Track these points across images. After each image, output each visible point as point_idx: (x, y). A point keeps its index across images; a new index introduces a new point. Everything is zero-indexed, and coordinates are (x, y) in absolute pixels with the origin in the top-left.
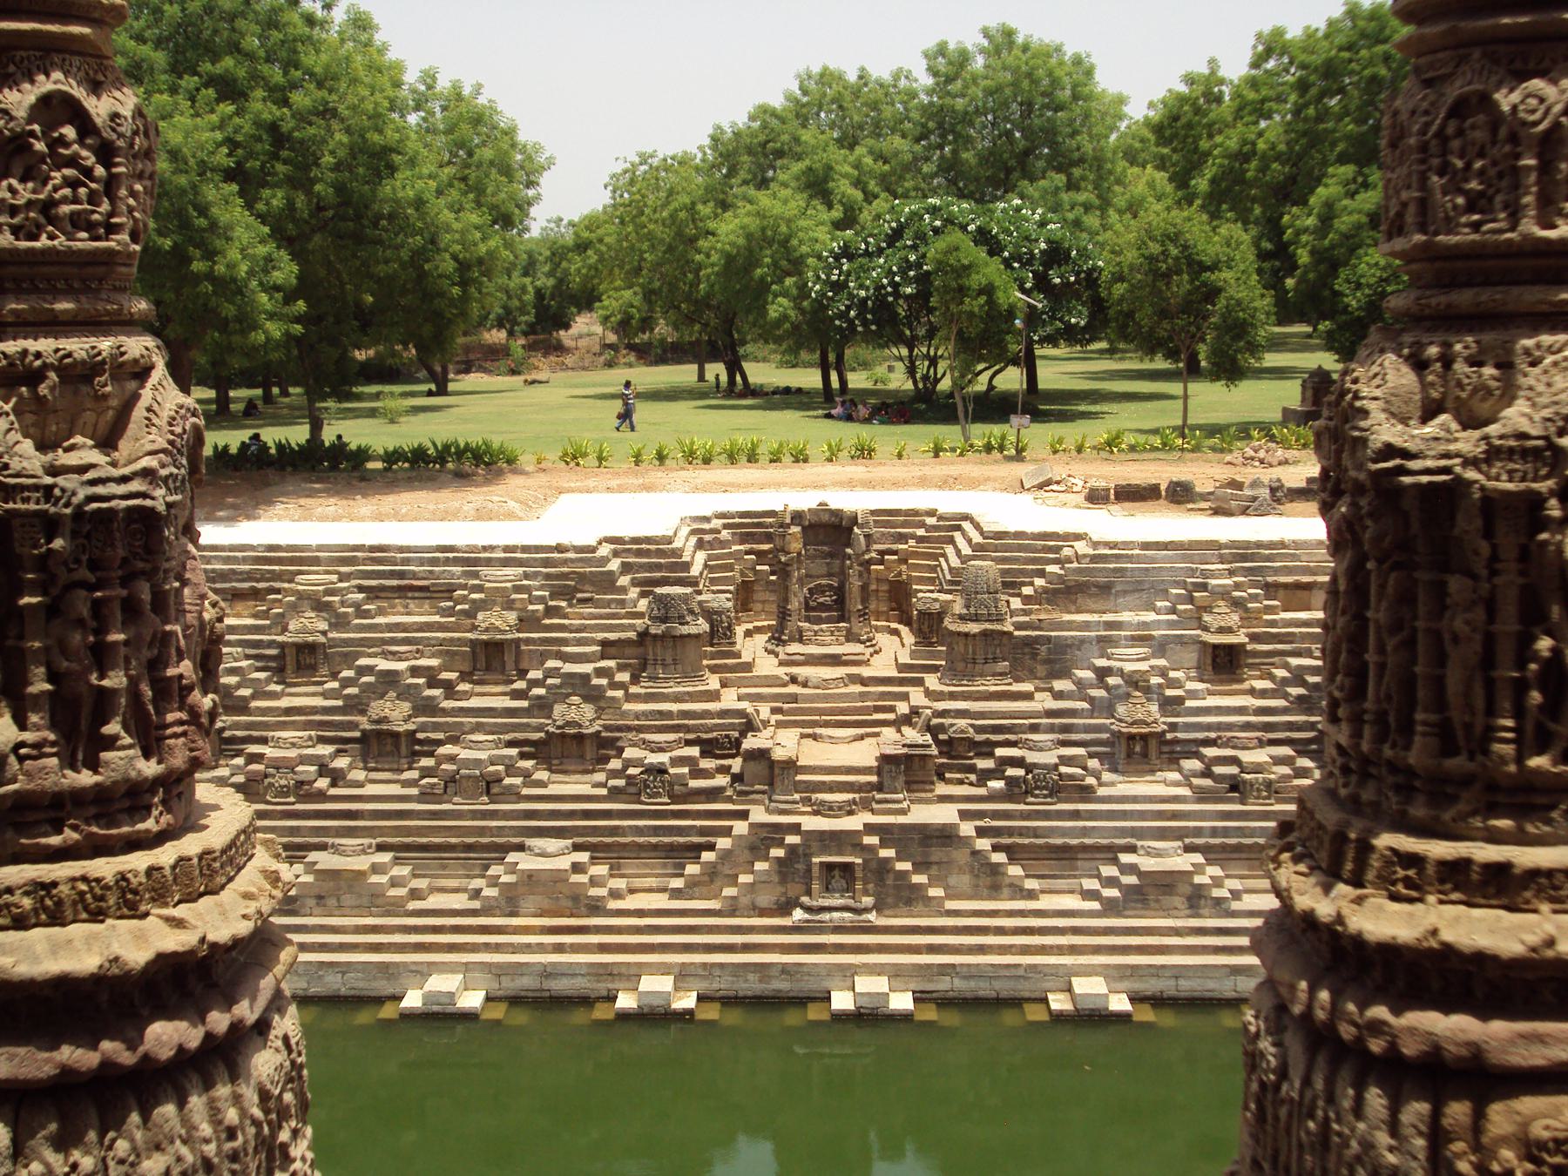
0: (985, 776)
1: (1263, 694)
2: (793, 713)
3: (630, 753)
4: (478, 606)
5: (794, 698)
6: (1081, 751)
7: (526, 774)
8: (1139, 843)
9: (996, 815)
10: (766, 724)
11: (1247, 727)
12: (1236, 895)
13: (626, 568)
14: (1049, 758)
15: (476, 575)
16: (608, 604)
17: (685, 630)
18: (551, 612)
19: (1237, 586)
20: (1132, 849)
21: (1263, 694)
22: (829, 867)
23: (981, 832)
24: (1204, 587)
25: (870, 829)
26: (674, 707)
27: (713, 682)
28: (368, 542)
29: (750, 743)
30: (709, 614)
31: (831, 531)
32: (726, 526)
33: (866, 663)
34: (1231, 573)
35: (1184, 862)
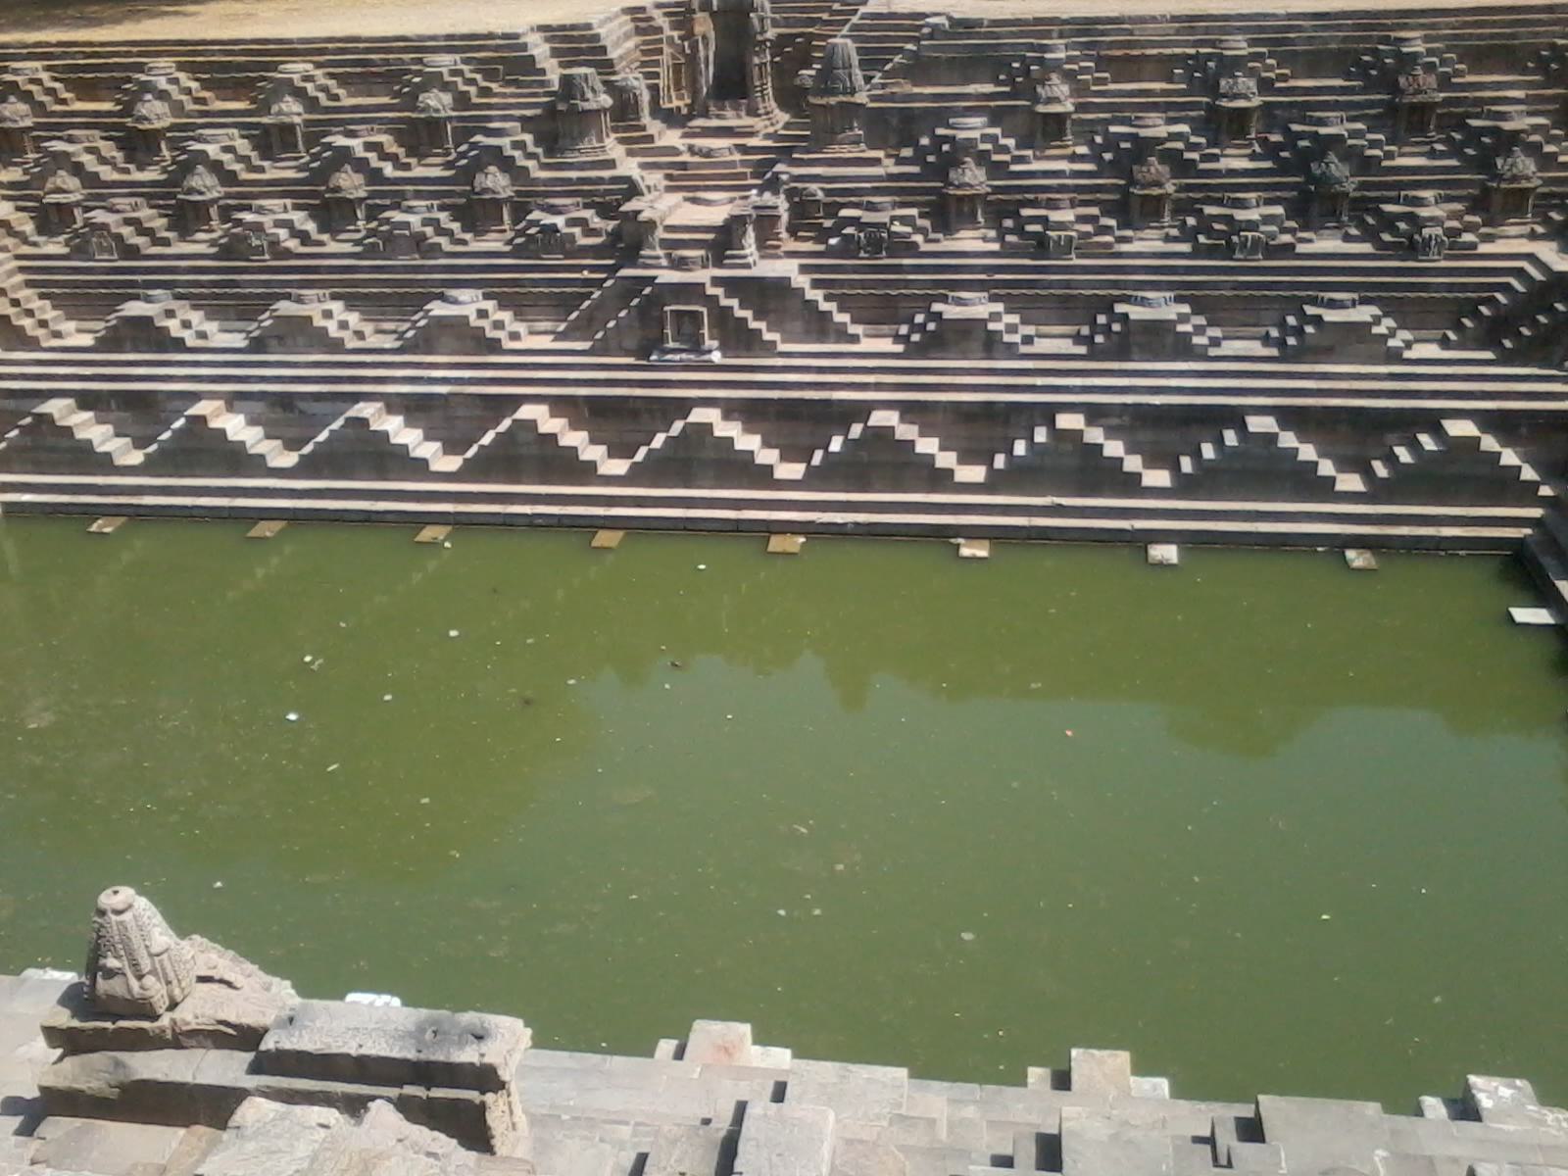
1: (1082, 158)
4: (424, 88)
5: (684, 166)
6: (914, 212)
8: (951, 294)
11: (1062, 189)
12: (1028, 340)
14: (882, 217)
15: (420, 61)
16: (530, 84)
17: (587, 106)
21: (1082, 158)
22: (677, 314)
24: (1041, 61)
25: (717, 281)
26: (574, 174)
28: (340, 34)
29: (627, 207)
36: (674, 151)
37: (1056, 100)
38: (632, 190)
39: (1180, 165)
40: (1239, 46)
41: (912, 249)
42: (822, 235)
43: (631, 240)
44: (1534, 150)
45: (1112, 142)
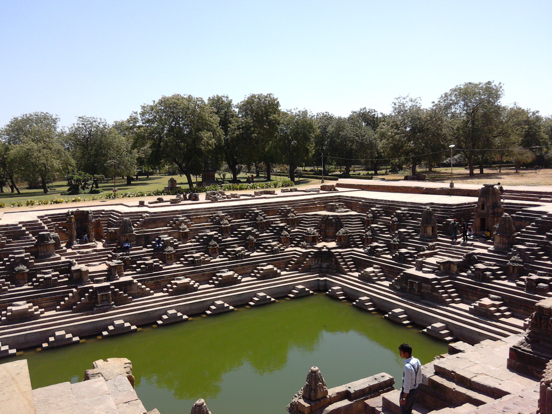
0: (136, 268)
2: (81, 260)
3: (38, 276)
5: (80, 257)
7: (8, 285)
9: (140, 277)
10: (75, 264)
11: (192, 249)
13: (27, 230)
14: (151, 261)
17: (49, 242)
18: (9, 242)
19: (185, 219)
20: (174, 280)
21: (194, 242)
23: (139, 281)
24: (178, 220)
25: (112, 285)
27: (58, 255)
29: (73, 268)
30: (55, 238)
31: (82, 216)
32: (49, 218)
33: (95, 247)
34: (183, 217)
35: (187, 280)
36: (74, 253)
37: (186, 229)
38: (71, 264)
39: (219, 241)
40: (221, 214)
41: (161, 269)
42: (134, 269)
43: (78, 278)
44: (286, 230)
45: (201, 237)
